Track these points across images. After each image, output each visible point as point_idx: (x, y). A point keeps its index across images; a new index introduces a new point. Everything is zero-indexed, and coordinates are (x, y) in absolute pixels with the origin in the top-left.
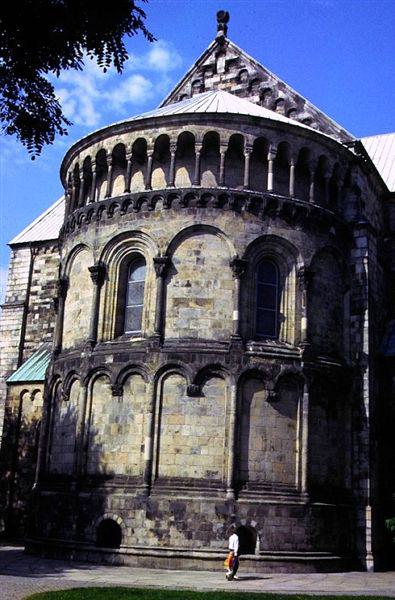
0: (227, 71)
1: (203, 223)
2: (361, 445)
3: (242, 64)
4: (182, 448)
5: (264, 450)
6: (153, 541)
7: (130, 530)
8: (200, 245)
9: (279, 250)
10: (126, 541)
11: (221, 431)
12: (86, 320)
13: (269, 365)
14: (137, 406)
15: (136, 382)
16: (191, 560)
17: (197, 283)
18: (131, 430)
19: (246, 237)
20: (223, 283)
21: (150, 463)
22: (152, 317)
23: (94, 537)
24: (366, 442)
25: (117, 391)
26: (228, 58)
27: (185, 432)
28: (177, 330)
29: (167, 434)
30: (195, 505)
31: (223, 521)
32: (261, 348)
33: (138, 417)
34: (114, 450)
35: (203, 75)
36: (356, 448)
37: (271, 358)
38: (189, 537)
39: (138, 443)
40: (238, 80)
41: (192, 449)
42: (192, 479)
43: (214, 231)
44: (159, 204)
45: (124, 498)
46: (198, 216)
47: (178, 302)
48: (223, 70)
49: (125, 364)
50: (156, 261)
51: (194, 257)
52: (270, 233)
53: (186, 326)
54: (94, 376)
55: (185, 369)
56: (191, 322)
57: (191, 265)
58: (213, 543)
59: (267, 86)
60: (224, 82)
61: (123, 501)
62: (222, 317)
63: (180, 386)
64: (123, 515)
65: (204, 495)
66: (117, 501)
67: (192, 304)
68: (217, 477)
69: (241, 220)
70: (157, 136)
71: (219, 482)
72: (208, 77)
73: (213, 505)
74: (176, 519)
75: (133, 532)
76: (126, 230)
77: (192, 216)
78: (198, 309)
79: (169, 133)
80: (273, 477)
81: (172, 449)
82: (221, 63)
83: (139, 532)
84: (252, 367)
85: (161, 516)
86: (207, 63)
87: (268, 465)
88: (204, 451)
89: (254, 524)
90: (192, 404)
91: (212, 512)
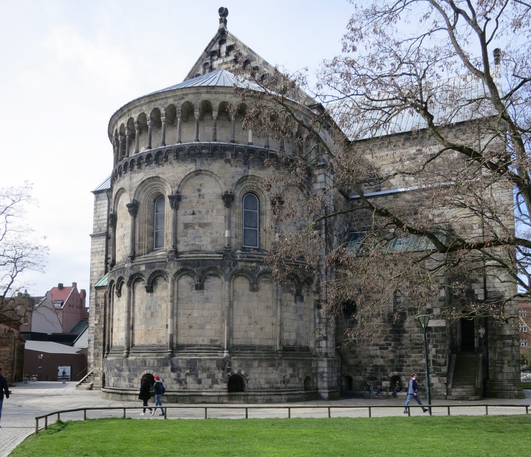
2: (320, 318)
5: (250, 324)
6: (176, 387)
8: (201, 185)
11: (219, 313)
12: (128, 241)
13: (251, 267)
14: (162, 298)
16: (201, 397)
17: (200, 212)
19: (233, 177)
20: (218, 210)
21: (172, 336)
22: (170, 237)
25: (150, 289)
27: (195, 315)
28: (187, 245)
29: (183, 316)
30: (203, 362)
31: (222, 371)
32: (245, 255)
33: (164, 306)
34: (149, 328)
36: (317, 321)
37: (252, 262)
38: (199, 382)
39: (164, 323)
42: (201, 345)
45: (156, 359)
47: (187, 226)
49: (153, 270)
50: (170, 197)
51: (197, 194)
52: (250, 174)
53: (193, 242)
54: (134, 280)
55: (193, 272)
56: (197, 240)
57: (195, 200)
58: (216, 386)
61: (156, 361)
63: (190, 284)
67: (196, 227)
68: (218, 343)
69: (228, 165)
73: (215, 361)
74: (190, 371)
78: (201, 230)
80: (256, 342)
81: (187, 326)
84: (240, 268)
85: (180, 370)
87: (253, 334)
88: (207, 327)
89: (243, 372)
90: (197, 295)
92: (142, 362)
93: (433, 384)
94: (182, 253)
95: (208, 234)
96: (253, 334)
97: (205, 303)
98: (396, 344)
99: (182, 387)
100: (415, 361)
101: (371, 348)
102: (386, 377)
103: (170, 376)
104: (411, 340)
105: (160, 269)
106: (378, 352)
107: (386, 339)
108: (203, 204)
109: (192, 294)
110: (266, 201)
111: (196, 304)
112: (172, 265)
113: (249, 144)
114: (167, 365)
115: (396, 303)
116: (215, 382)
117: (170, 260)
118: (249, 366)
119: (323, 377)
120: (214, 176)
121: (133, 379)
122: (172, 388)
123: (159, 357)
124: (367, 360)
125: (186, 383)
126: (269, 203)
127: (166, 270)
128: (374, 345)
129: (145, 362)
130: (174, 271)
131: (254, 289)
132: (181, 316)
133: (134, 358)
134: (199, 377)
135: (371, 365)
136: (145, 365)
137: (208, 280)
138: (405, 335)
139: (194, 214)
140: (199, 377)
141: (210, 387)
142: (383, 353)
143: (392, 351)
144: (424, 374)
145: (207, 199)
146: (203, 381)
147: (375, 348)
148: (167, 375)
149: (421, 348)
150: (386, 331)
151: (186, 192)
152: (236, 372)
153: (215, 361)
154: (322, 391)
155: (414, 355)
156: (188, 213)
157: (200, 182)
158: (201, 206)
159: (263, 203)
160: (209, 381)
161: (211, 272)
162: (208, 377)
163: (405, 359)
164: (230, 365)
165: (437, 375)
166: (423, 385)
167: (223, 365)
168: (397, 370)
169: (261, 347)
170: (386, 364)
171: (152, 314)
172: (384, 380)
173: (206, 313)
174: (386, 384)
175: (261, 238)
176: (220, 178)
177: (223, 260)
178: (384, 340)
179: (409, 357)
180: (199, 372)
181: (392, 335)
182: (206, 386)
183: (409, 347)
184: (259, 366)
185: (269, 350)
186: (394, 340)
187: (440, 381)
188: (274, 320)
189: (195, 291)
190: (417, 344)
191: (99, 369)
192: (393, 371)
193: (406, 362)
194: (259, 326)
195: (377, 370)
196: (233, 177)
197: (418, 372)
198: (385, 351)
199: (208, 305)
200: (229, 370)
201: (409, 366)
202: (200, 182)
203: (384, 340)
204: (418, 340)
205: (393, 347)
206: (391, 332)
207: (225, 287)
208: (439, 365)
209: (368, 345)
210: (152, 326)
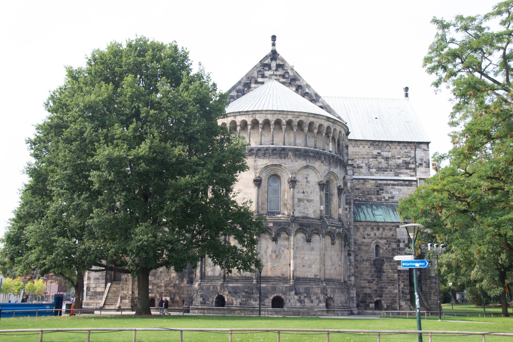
0: (276, 70)
1: (310, 165)
3: (286, 68)
4: (305, 265)
5: (331, 266)
6: (298, 305)
7: (288, 300)
8: (308, 175)
9: (332, 178)
10: (286, 305)
11: (318, 257)
13: (334, 230)
15: (284, 235)
17: (307, 192)
18: (283, 256)
19: (325, 172)
20: (316, 192)
23: (270, 304)
24: (353, 261)
26: (278, 63)
27: (306, 258)
28: (300, 213)
30: (314, 289)
31: (323, 295)
35: (263, 69)
36: (348, 264)
37: (334, 226)
38: (312, 302)
40: (283, 76)
41: (309, 265)
43: (313, 168)
44: (290, 154)
46: (308, 161)
47: (300, 200)
48: (275, 69)
49: (280, 227)
51: (305, 180)
53: (303, 211)
55: (307, 231)
56: (306, 210)
57: (305, 184)
58: (320, 304)
59: (300, 84)
60: (276, 75)
61: (284, 288)
62: (316, 208)
63: (303, 238)
64: (285, 294)
65: (316, 285)
66: (281, 288)
67: (305, 202)
68: (318, 277)
69: (323, 164)
70: (287, 119)
71: (319, 279)
72: (266, 70)
73: (320, 289)
75: (289, 301)
76: (274, 163)
77: (305, 161)
78: (308, 204)
79: (294, 119)
80: (334, 277)
81: (301, 265)
82: (274, 64)
83: (292, 301)
84: (329, 230)
85: (301, 294)
86: (266, 62)
87: (332, 272)
88: (313, 266)
89: (332, 296)
90: (307, 245)
91: (319, 292)
92: (272, 288)
93: (402, 306)
94: (298, 217)
95: (311, 207)
96: (332, 272)
97: (311, 251)
98: (378, 280)
99: (302, 305)
100: (390, 291)
101: (362, 281)
102: (372, 301)
103: (294, 298)
104: (387, 278)
105: (285, 227)
106: (367, 285)
107: (372, 276)
108: (309, 187)
109: (304, 245)
110: (334, 187)
111: (307, 251)
112: (293, 226)
113: (330, 151)
114: (292, 290)
115: (377, 254)
116: (320, 302)
117: (292, 222)
118: (334, 292)
119: (353, 300)
120: (315, 170)
121: (264, 300)
122: (295, 305)
123: (285, 285)
124: (359, 289)
125: (304, 302)
126: (336, 189)
127: (290, 228)
128: (364, 280)
129: (275, 288)
130: (295, 230)
131: (333, 244)
132: (298, 258)
133: (265, 285)
134: (312, 299)
135: (362, 293)
136: (275, 290)
137: (313, 236)
138: (384, 274)
139: (304, 193)
140: (312, 299)
141: (318, 305)
142: (370, 285)
143: (376, 284)
144: (396, 300)
145: (311, 184)
146: (314, 301)
147: (365, 281)
148: (292, 297)
149: (394, 283)
150: (372, 271)
151: (299, 178)
152: (329, 296)
153: (320, 289)
154: (353, 309)
155: (389, 287)
156: (300, 192)
157: (307, 173)
158: (308, 188)
159: (333, 188)
160: (317, 301)
161: (315, 232)
162: (317, 299)
163: (384, 290)
164: (327, 291)
165: (405, 300)
166: (395, 307)
167: (324, 291)
168: (379, 296)
169: (336, 280)
170: (372, 293)
171: (277, 256)
172: (371, 303)
173: (312, 257)
174: (372, 305)
175: (332, 210)
176: (319, 172)
177: (322, 224)
178: (371, 277)
179: (387, 288)
180: (312, 295)
181: (376, 274)
182: (316, 305)
183: (386, 282)
184: (338, 292)
185: (339, 281)
186: (377, 277)
187: (406, 304)
188: (340, 263)
189: (306, 243)
190: (391, 280)
191: (128, 293)
192: (376, 297)
193: (385, 292)
194: (335, 267)
195: (366, 296)
196: (325, 172)
197: (392, 298)
198: (371, 284)
199: (313, 252)
200: (326, 294)
201: (386, 294)
202: (307, 173)
203: (371, 277)
204: (392, 277)
205: (376, 282)
206: (375, 272)
207: (322, 241)
208: (406, 294)
209: (360, 280)
210: (277, 264)
